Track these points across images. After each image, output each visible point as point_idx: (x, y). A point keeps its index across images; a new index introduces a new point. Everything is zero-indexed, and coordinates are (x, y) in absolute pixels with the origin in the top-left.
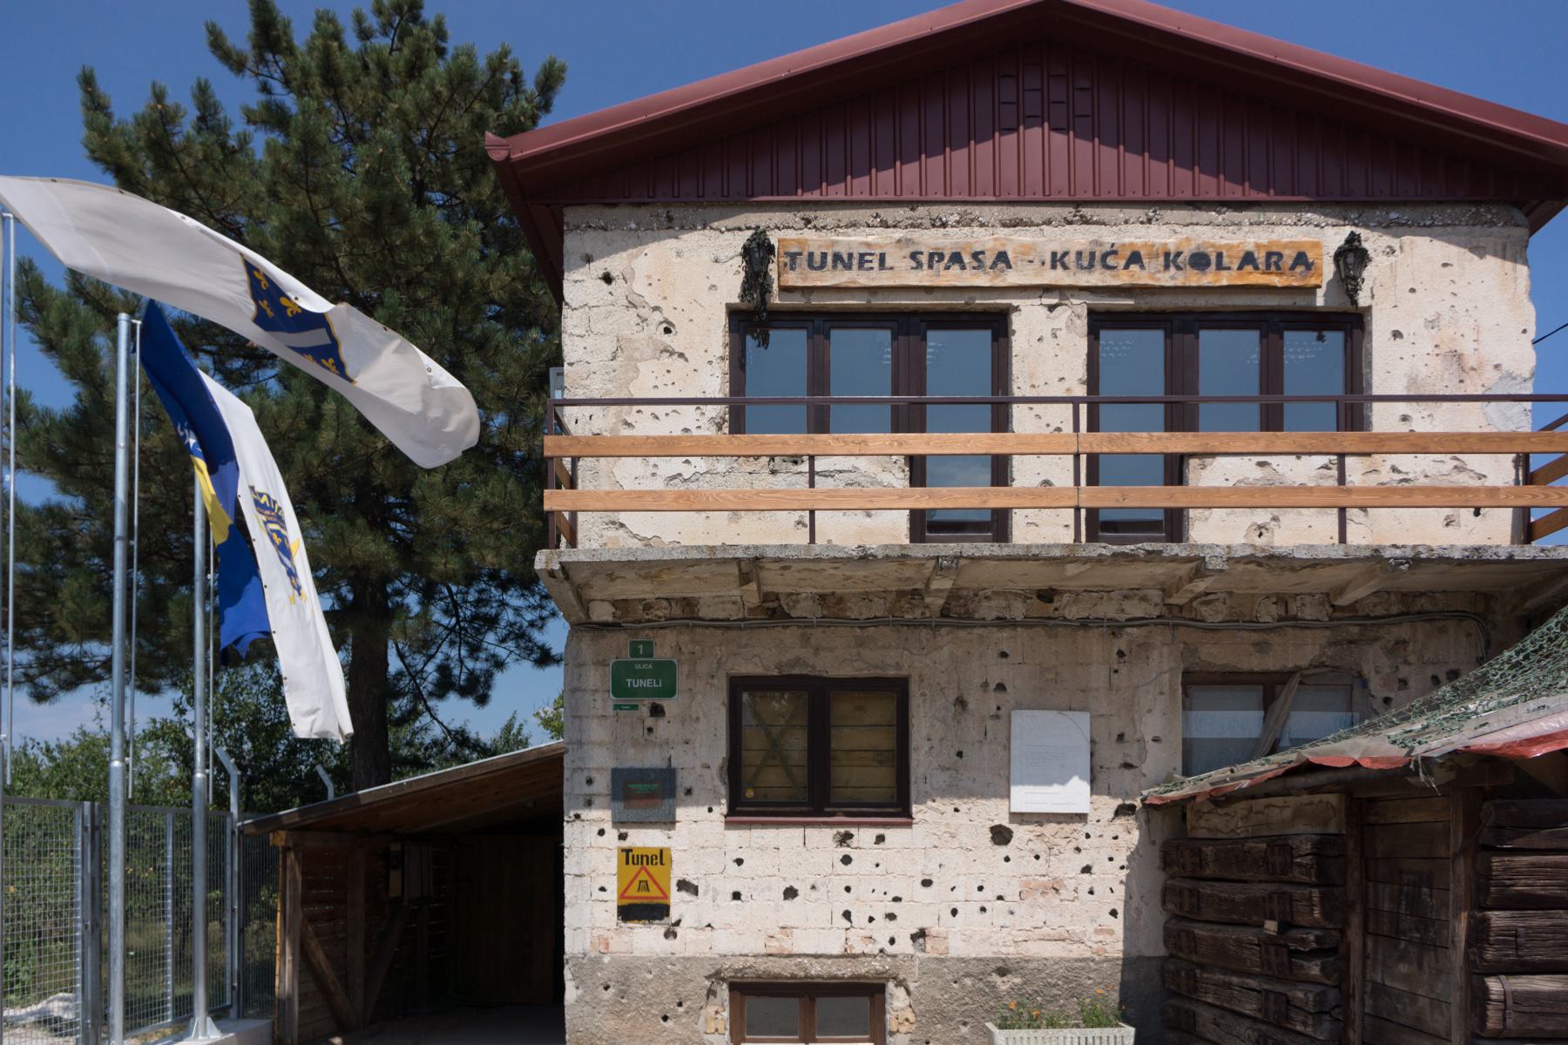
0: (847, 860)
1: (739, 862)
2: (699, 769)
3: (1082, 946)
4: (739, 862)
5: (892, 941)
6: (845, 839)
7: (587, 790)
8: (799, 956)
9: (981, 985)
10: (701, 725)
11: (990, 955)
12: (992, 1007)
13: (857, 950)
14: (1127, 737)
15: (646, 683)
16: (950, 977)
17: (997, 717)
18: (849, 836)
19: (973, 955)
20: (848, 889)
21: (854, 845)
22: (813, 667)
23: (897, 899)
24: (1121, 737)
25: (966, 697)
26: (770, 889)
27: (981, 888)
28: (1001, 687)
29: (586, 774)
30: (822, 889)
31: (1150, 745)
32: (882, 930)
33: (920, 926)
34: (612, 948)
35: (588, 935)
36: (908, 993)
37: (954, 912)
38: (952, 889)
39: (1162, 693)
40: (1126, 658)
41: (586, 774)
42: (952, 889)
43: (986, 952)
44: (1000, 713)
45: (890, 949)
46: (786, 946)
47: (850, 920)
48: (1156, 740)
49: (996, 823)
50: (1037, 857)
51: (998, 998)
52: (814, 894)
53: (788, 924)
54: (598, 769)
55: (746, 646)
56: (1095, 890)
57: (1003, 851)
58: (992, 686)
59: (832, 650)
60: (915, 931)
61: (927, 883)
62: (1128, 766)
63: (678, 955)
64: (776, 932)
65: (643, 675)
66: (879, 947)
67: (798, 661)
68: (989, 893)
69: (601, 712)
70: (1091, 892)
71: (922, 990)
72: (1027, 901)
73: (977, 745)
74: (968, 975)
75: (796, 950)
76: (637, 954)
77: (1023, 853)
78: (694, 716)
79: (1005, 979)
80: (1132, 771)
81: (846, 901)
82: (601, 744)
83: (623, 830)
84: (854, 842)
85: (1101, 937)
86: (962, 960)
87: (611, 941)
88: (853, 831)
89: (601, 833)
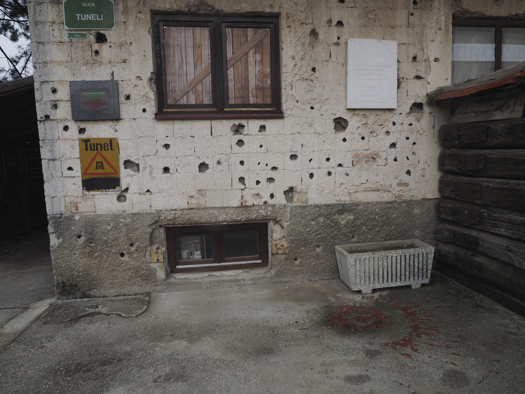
0: (240, 143)
1: (167, 146)
2: (134, 80)
3: (390, 194)
4: (167, 146)
5: (272, 196)
6: (238, 129)
7: (52, 97)
8: (211, 208)
9: (329, 222)
10: (133, 48)
11: (334, 202)
12: (336, 235)
13: (249, 203)
14: (418, 59)
15: (91, 17)
16: (309, 218)
17: (338, 44)
18: (242, 126)
19: (324, 203)
21: (245, 133)
23: (274, 168)
24: (415, 58)
26: (189, 165)
27: (328, 159)
28: (340, 24)
29: (51, 85)
30: (225, 164)
31: (433, 63)
32: (265, 190)
33: (290, 185)
34: (81, 208)
35: (62, 202)
36: (282, 227)
37: (311, 176)
38: (310, 161)
39: (440, 29)
40: (418, 6)
41: (51, 85)
42: (310, 161)
43: (331, 200)
44: (340, 41)
45: (270, 201)
46: (202, 203)
47: (244, 184)
48: (436, 60)
49: (338, 116)
50: (363, 138)
51: (339, 229)
52: (220, 167)
53: (203, 188)
54: (61, 82)
56: (398, 158)
57: (342, 135)
58: (334, 23)
60: (287, 189)
61: (294, 157)
62: (418, 77)
63: (128, 212)
66: (263, 200)
68: (333, 163)
69: (58, 39)
70: (395, 160)
71: (292, 227)
72: (357, 167)
73: (325, 63)
74: (320, 215)
75: (208, 205)
76: (98, 212)
77: (354, 136)
78: (128, 42)
79: (343, 216)
80: (422, 80)
81: (241, 171)
82: (61, 63)
83: (82, 125)
84: (245, 131)
85: (401, 188)
86: (317, 206)
87: (79, 205)
88: (244, 122)
89: (66, 128)
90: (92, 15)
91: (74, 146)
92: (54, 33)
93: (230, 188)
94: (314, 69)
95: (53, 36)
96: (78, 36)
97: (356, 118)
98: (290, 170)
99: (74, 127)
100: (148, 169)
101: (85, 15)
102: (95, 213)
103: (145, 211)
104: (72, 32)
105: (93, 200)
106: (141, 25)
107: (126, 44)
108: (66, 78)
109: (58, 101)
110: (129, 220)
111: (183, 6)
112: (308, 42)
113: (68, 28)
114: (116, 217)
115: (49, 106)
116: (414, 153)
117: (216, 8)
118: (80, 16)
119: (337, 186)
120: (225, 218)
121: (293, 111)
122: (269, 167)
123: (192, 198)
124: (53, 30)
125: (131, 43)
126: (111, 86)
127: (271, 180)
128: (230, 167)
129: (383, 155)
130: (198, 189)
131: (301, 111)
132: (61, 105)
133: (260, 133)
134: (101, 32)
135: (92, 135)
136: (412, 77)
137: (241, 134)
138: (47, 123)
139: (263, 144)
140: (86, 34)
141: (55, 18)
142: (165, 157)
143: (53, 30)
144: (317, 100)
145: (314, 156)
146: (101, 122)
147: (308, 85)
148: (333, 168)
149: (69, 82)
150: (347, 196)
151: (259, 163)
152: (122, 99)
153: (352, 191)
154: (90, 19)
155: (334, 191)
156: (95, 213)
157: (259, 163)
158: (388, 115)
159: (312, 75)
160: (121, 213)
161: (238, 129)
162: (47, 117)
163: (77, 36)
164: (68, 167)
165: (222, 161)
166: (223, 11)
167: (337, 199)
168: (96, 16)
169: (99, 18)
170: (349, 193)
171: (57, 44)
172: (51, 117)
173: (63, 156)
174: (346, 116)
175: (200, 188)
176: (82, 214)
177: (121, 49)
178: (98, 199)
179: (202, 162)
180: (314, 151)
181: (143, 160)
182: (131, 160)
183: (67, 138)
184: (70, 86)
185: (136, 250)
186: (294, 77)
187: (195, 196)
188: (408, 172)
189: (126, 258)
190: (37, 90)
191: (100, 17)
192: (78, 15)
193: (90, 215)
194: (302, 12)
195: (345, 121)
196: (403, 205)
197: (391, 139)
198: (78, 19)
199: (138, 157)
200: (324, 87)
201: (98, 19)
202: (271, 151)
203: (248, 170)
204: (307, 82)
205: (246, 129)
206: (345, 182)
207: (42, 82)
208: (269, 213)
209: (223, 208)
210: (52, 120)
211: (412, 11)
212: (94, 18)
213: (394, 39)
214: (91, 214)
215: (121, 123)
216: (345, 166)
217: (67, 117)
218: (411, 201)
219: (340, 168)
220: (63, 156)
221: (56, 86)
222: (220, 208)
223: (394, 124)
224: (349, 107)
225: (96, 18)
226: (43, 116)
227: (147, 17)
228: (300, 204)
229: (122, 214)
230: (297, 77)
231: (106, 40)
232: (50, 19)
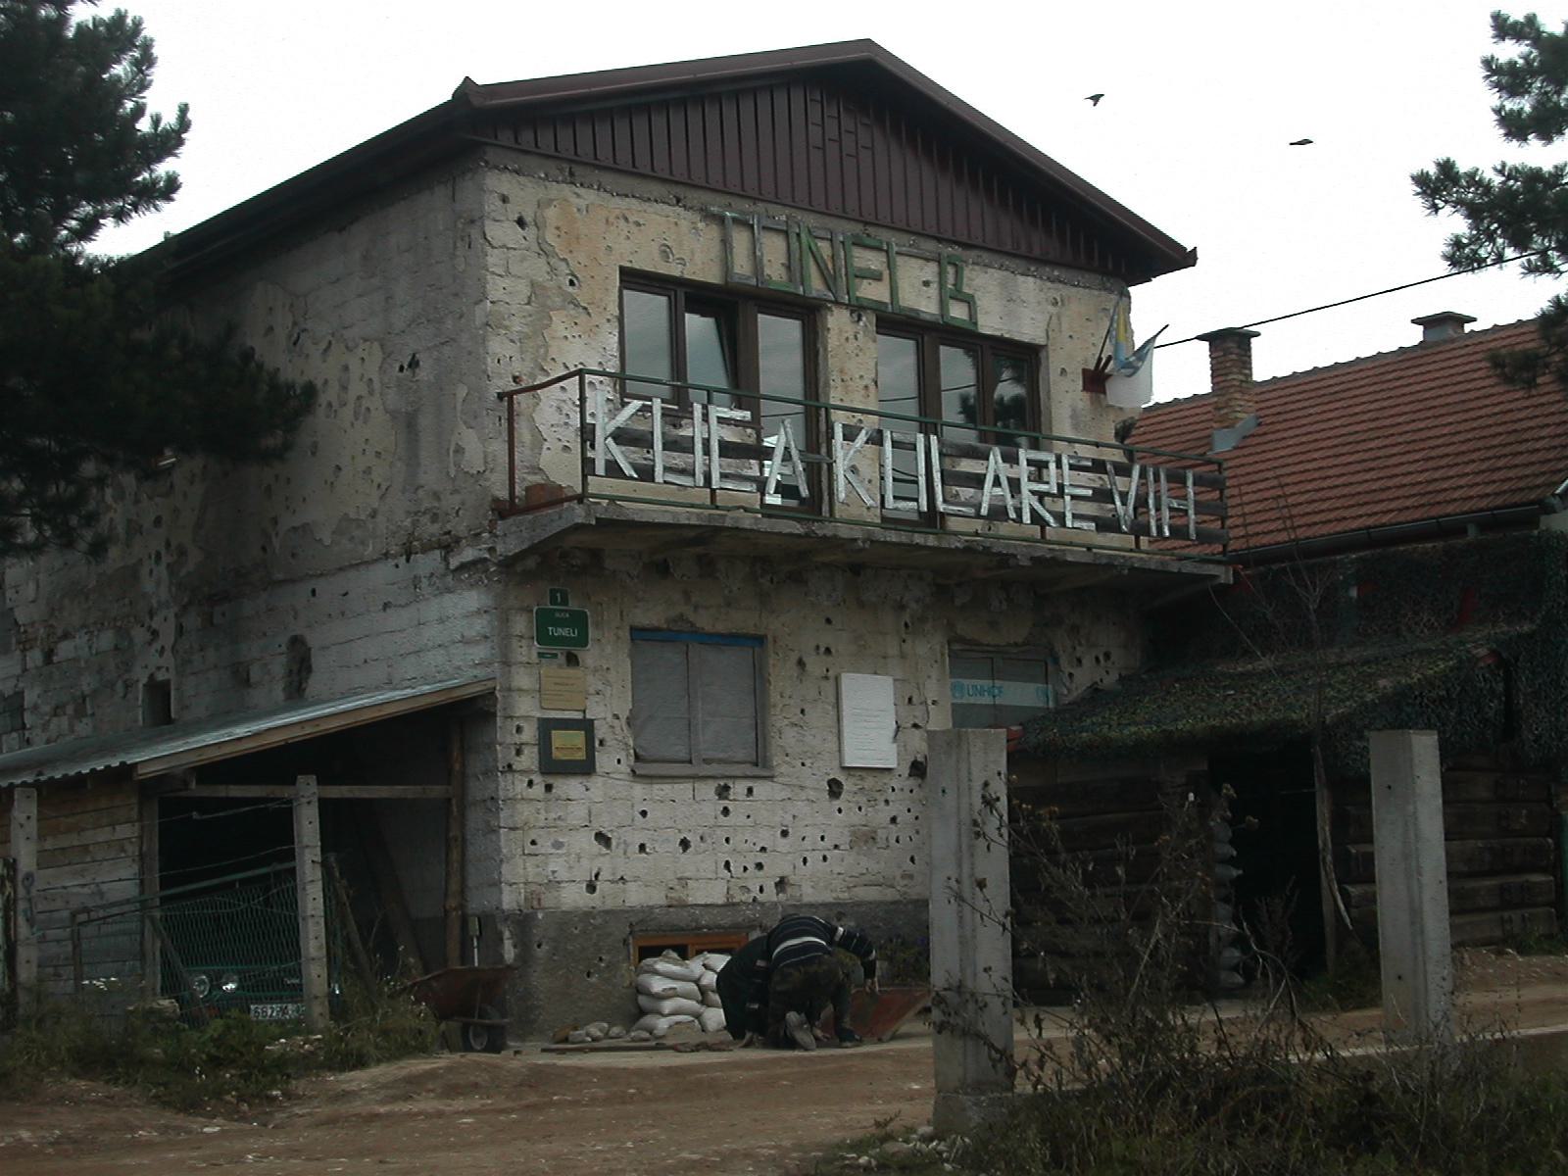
1: (644, 813)
4: (644, 813)
6: (723, 792)
7: (517, 739)
10: (612, 676)
11: (831, 900)
17: (827, 678)
18: (727, 788)
20: (727, 840)
21: (731, 798)
22: (692, 625)
23: (763, 849)
24: (910, 700)
31: (931, 707)
34: (546, 903)
37: (805, 861)
44: (830, 673)
45: (760, 897)
47: (730, 871)
48: (934, 702)
50: (860, 809)
54: (526, 718)
57: (837, 804)
58: (822, 650)
61: (785, 834)
62: (915, 726)
64: (673, 883)
68: (828, 843)
70: (897, 841)
75: (691, 900)
83: (550, 780)
85: (905, 882)
87: (543, 896)
89: (530, 783)
94: (802, 711)
97: (852, 780)
99: (537, 779)
108: (533, 714)
110: (599, 921)
114: (588, 915)
116: (918, 832)
125: (608, 669)
129: (881, 834)
130: (679, 875)
132: (526, 751)
136: (909, 725)
137: (727, 798)
138: (509, 776)
144: (809, 754)
145: (807, 832)
158: (886, 778)
161: (723, 792)
162: (510, 766)
165: (706, 837)
167: (834, 895)
170: (848, 888)
174: (841, 778)
185: (608, 967)
188: (912, 859)
189: (593, 979)
195: (839, 784)
196: (910, 906)
197: (891, 810)
204: (796, 729)
211: (904, 636)
213: (887, 674)
215: (594, 779)
216: (842, 847)
218: (918, 901)
223: (893, 790)
227: (626, 634)
230: (786, 722)
231: (577, 663)
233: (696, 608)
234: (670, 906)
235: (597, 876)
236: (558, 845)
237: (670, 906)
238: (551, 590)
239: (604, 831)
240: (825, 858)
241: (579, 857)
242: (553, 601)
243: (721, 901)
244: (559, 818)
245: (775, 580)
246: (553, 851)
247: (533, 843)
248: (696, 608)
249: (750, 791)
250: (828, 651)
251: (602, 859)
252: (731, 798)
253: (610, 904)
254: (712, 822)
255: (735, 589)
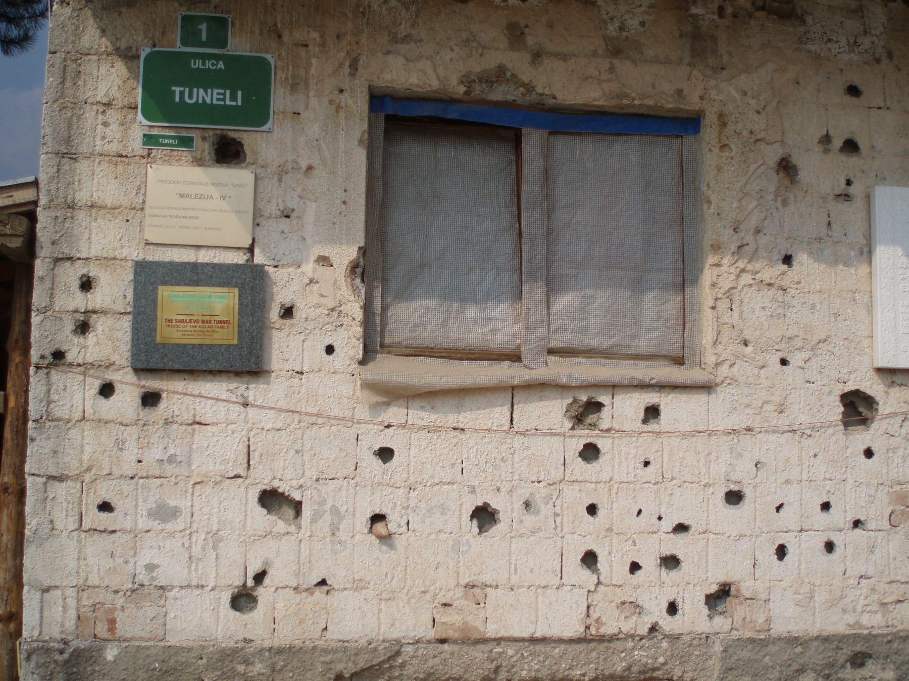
0: (590, 452)
4: (385, 454)
5: (672, 609)
7: (80, 301)
8: (498, 641)
13: (608, 629)
15: (212, 96)
17: (847, 197)
18: (595, 406)
20: (592, 509)
21: (605, 425)
22: (529, 88)
23: (681, 528)
25: (794, 160)
27: (826, 506)
28: (851, 146)
29: (80, 269)
30: (546, 510)
33: (722, 579)
34: (125, 627)
35: (72, 603)
37: (781, 552)
38: (778, 509)
41: (80, 269)
42: (778, 509)
44: (852, 190)
45: (668, 624)
49: (850, 387)
52: (530, 520)
54: (109, 261)
55: (407, 39)
57: (861, 438)
58: (838, 143)
59: (564, 57)
60: (714, 588)
61: (734, 497)
64: (456, 596)
65: (207, 80)
67: (500, 75)
68: (840, 516)
69: (114, 148)
75: (492, 630)
76: (173, 640)
78: (304, 164)
83: (153, 384)
84: (605, 418)
87: (119, 616)
89: (107, 390)
90: (215, 91)
91: (123, 442)
92: (108, 130)
93: (557, 581)
95: (104, 138)
96: (167, 141)
98: (723, 534)
100: (328, 517)
101: (195, 90)
102: (162, 644)
103: (307, 642)
104: (155, 132)
105: (162, 602)
106: (343, 122)
107: (296, 168)
108: (124, 253)
109: (94, 312)
110: (258, 668)
111: (454, 80)
112: (772, 188)
113: (146, 122)
115: (69, 326)
117: (539, 90)
118: (182, 94)
119: (851, 581)
120: (538, 671)
121: (735, 369)
122: (668, 524)
123: (450, 610)
124: (105, 124)
125: (310, 168)
126: (247, 280)
127: (671, 562)
128: (559, 520)
130: (464, 581)
131: (756, 371)
132: (100, 325)
133: (646, 428)
134: (232, 135)
135: (177, 413)
137: (593, 426)
139: (651, 459)
140: (191, 140)
141: (115, 93)
142: (379, 484)
143: (105, 124)
144: (798, 343)
145: (789, 495)
146: (210, 377)
147: (773, 300)
148: (840, 530)
149: (130, 264)
150: (876, 612)
151: (640, 512)
152: (274, 314)
153: (893, 598)
154: (208, 101)
155: (842, 597)
156: (162, 644)
157: (640, 512)
159: (783, 274)
160: (239, 645)
162: (59, 355)
163: (167, 141)
164: (99, 501)
165: (538, 501)
166: (554, 97)
168: (224, 94)
169: (231, 100)
170: (883, 604)
171: (110, 162)
172: (69, 357)
173: (89, 469)
174: (873, 387)
175: (473, 578)
176: (127, 644)
177: (280, 180)
178: (176, 599)
179: (480, 504)
180: (788, 482)
181: (315, 492)
182: (280, 490)
183: (105, 417)
184: (136, 274)
186: (738, 276)
187: (455, 604)
190: (42, 279)
191: (233, 98)
192: (177, 90)
193: (148, 648)
194: (758, 112)
195: (870, 401)
198: (177, 100)
199: (301, 482)
200: (813, 306)
201: (228, 102)
202: (673, 479)
203: (610, 530)
205: (605, 412)
206: (871, 572)
207: (57, 260)
208: (661, 660)
209: (533, 640)
210: (71, 365)
212: (218, 100)
214: (152, 643)
216: (871, 525)
217: (115, 358)
219: (857, 531)
220: (89, 469)
221: (93, 271)
222: (523, 640)
224: (881, 364)
225: (224, 100)
226: (47, 353)
227: (359, 103)
228: (748, 634)
229: (242, 649)
232: (101, 96)
233: (537, 56)
234: (443, 641)
235: (260, 578)
236: (164, 513)
237: (443, 641)
238: (184, 18)
239: (283, 488)
240: (830, 547)
241: (215, 538)
242: (190, 37)
243: (572, 628)
244: (172, 459)
245: (729, 10)
246: (155, 524)
247: (105, 507)
248: (537, 56)
249: (652, 412)
250: (851, 146)
251: (271, 542)
252: (605, 425)
253: (286, 635)
254: (556, 474)
255: (633, 23)
